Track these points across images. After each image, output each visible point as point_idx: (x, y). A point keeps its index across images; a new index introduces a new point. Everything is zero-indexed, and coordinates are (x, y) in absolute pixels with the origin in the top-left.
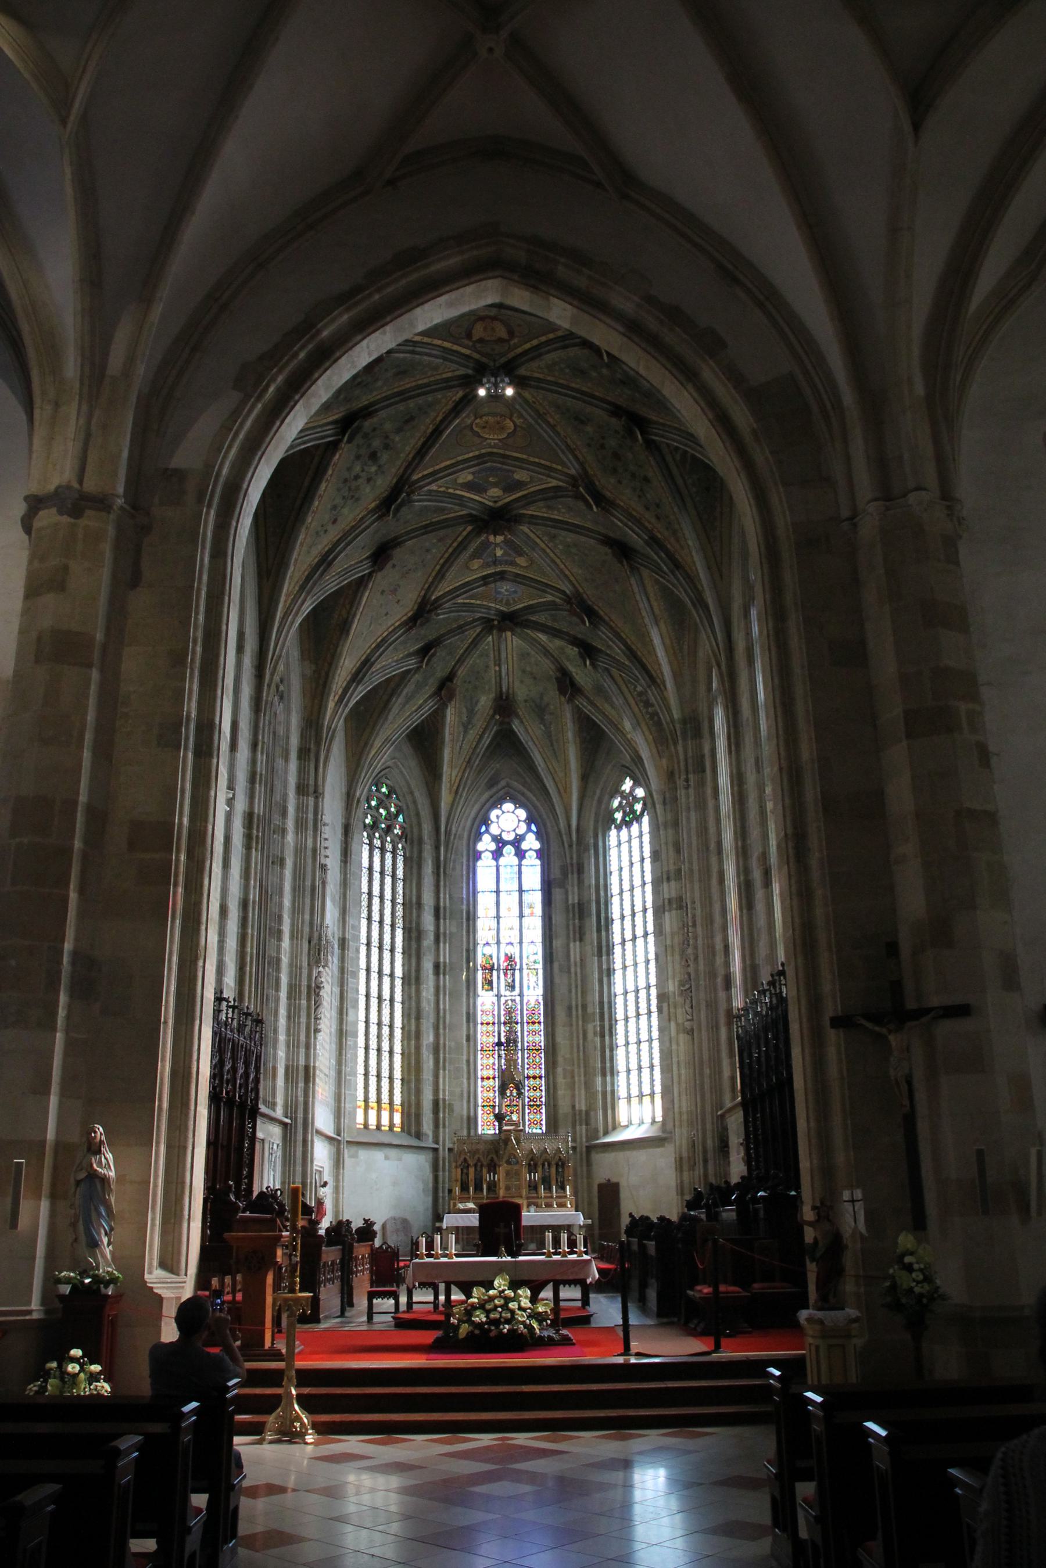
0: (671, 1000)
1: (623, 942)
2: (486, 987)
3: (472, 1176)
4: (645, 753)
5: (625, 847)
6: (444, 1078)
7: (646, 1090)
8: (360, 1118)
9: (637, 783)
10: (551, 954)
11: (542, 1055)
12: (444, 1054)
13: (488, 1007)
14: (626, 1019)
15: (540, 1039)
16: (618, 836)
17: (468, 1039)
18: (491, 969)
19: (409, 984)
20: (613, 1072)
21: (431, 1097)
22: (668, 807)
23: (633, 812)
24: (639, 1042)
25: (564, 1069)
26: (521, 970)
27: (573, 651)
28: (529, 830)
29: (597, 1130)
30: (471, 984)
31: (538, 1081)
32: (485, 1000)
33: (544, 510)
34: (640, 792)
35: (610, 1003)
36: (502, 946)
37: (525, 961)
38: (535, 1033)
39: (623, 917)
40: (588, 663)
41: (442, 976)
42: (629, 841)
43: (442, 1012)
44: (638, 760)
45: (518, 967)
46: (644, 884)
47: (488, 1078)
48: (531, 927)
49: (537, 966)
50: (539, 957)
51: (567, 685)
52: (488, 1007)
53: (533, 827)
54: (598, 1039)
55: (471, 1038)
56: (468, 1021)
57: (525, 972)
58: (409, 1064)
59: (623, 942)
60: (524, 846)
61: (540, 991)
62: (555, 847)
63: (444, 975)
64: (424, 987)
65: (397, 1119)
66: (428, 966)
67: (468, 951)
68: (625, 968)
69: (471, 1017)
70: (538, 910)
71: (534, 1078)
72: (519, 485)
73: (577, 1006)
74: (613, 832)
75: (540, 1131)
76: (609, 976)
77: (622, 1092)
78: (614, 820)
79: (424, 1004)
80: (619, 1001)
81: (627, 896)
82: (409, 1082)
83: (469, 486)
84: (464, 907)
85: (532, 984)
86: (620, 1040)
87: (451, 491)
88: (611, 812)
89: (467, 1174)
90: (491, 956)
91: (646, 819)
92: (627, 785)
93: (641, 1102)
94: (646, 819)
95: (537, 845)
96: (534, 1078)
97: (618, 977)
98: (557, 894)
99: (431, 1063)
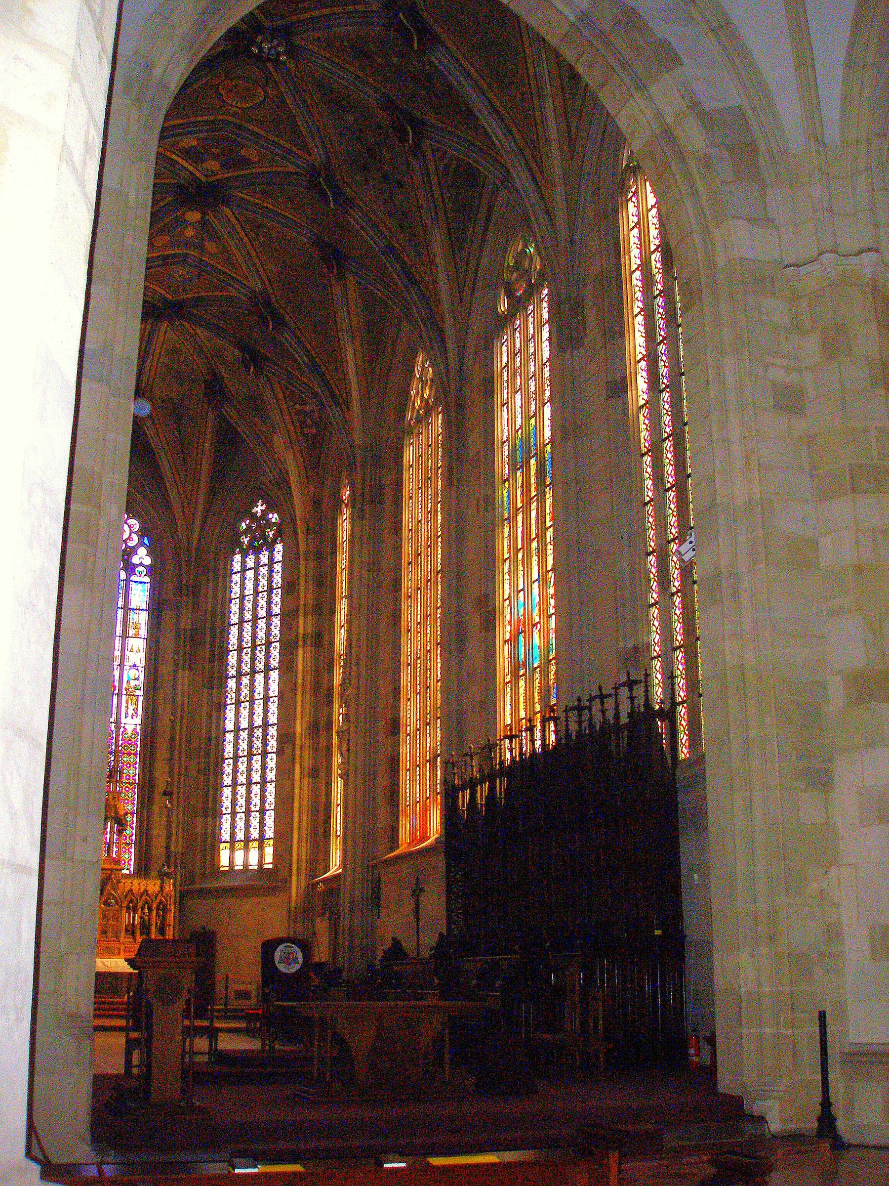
0: (298, 741)
1: (239, 675)
4: (294, 479)
5: (250, 574)
7: (255, 834)
9: (271, 506)
11: (136, 790)
14: (236, 758)
16: (243, 563)
20: (217, 814)
22: (311, 536)
23: (265, 538)
24: (249, 783)
26: (119, 695)
27: (233, 354)
28: (141, 543)
33: (258, 195)
34: (274, 517)
35: (217, 738)
37: (125, 685)
39: (240, 649)
40: (252, 369)
42: (256, 568)
44: (284, 482)
45: (116, 692)
46: (270, 615)
48: (135, 649)
49: (138, 693)
50: (141, 683)
51: (214, 389)
53: (146, 541)
57: (124, 698)
59: (239, 675)
60: (135, 560)
61: (138, 720)
62: (171, 566)
68: (238, 703)
70: (143, 632)
72: (245, 162)
73: (181, 739)
74: (238, 558)
75: (127, 872)
76: (219, 710)
77: (226, 835)
78: (239, 544)
80: (230, 737)
81: (248, 627)
83: (187, 153)
85: (131, 712)
86: (227, 781)
87: (168, 154)
88: (238, 534)
91: (279, 547)
92: (259, 509)
93: (246, 848)
94: (279, 547)
95: (148, 561)
97: (230, 714)
98: (169, 617)
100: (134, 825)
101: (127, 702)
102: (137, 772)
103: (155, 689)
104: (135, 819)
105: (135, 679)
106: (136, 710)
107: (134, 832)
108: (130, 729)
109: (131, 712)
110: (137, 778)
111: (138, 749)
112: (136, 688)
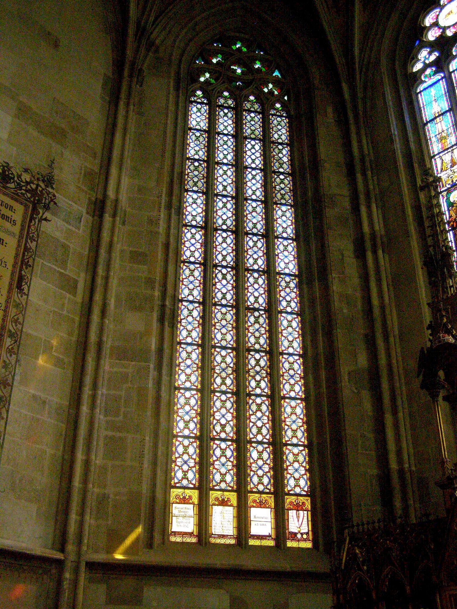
6: (396, 425)
8: (183, 521)
43: (377, 312)
58: (320, 416)
65: (299, 523)
66: (340, 245)
79: (337, 303)
84: (398, 146)
99: (368, 406)
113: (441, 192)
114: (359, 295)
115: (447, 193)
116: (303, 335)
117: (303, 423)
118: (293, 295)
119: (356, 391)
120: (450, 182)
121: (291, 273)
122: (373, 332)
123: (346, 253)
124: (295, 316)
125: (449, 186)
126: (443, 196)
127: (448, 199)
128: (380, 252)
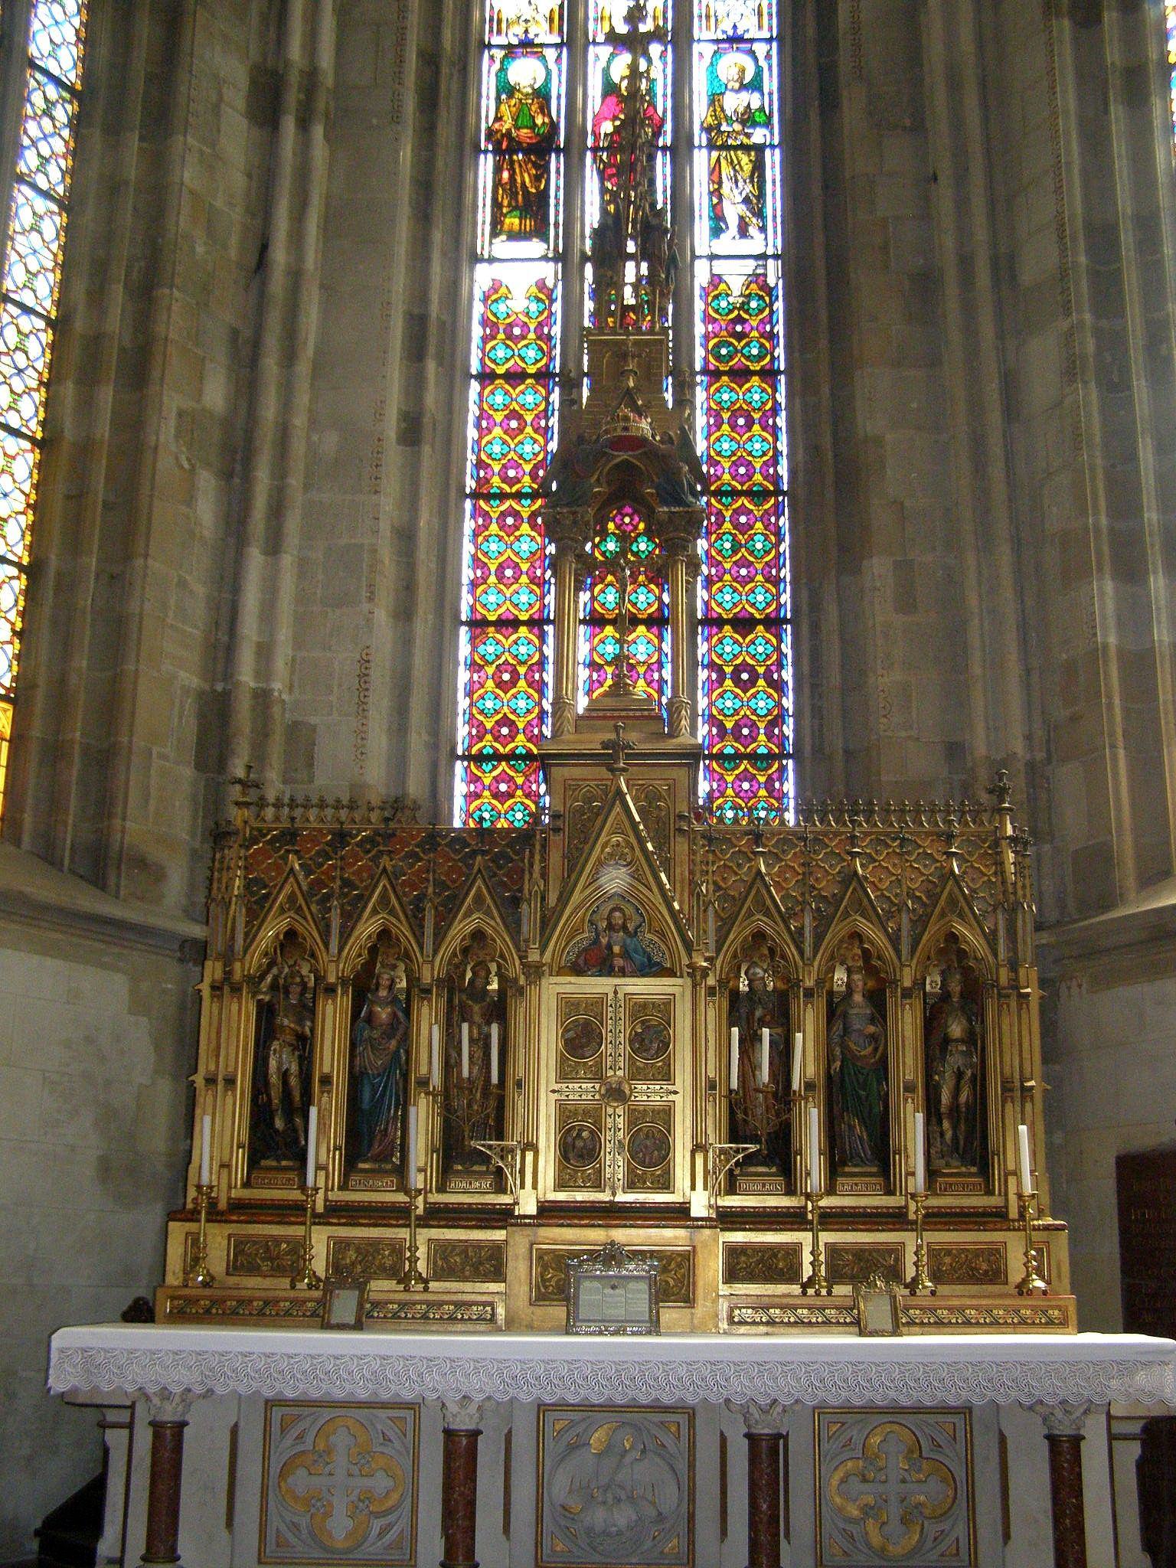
2: (512, 222)
3: (331, 1056)
10: (827, 75)
11: (784, 522)
12: (281, 472)
13: (519, 303)
15: (773, 450)
17: (412, 431)
18: (542, 147)
19: (114, 130)
21: (190, 679)
25: (904, 568)
26: (681, 151)
29: (1096, 861)
30: (438, 199)
31: (760, 643)
32: (513, 273)
36: (599, 56)
38: (742, 418)
41: (289, 125)
45: (666, 139)
47: (507, 624)
49: (759, 136)
52: (519, 303)
54: (1089, 395)
55: (426, 430)
56: (416, 351)
57: (701, 161)
58: (78, 497)
61: (768, 240)
63: (304, 125)
64: (186, 146)
67: (431, 59)
69: (431, 335)
71: (744, 624)
73: (966, 262)
79: (182, 220)
82: (67, 585)
85: (733, 211)
89: (304, 1046)
90: (542, 96)
96: (744, 624)
99: (206, 511)
100: (788, 675)
101: (715, 171)
102: (783, 446)
103: (829, 103)
104: (787, 649)
105: (743, 87)
106: (755, 204)
107: (788, 703)
108: (736, 276)
109: (733, 211)
110: (783, 469)
111: (780, 351)
112: (747, 118)
113: (490, 46)
114: (236, 216)
115: (506, 56)
116: (67, 266)
117: (28, 505)
118: (59, 146)
119: (186, 466)
120: (519, 30)
121: (64, 79)
122: (259, 329)
123: (228, 93)
124: (55, 208)
125: (515, 42)
126: (492, 58)
127: (503, 69)
128: (318, 131)
